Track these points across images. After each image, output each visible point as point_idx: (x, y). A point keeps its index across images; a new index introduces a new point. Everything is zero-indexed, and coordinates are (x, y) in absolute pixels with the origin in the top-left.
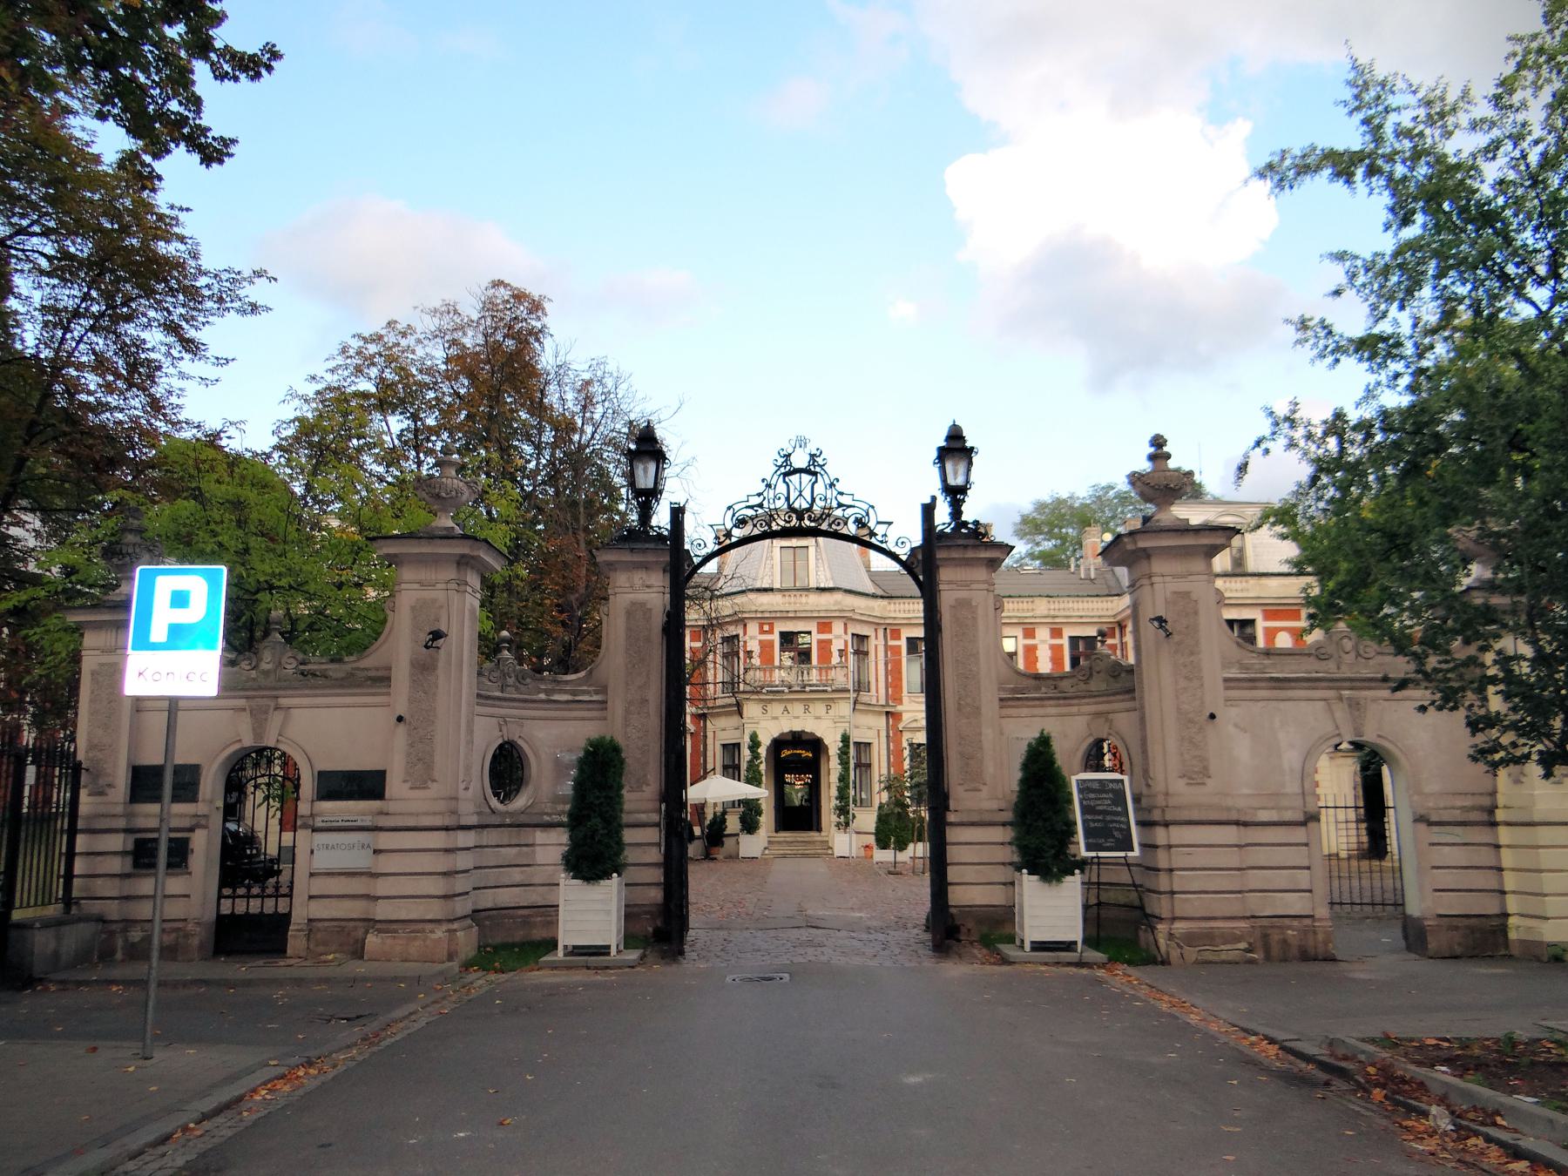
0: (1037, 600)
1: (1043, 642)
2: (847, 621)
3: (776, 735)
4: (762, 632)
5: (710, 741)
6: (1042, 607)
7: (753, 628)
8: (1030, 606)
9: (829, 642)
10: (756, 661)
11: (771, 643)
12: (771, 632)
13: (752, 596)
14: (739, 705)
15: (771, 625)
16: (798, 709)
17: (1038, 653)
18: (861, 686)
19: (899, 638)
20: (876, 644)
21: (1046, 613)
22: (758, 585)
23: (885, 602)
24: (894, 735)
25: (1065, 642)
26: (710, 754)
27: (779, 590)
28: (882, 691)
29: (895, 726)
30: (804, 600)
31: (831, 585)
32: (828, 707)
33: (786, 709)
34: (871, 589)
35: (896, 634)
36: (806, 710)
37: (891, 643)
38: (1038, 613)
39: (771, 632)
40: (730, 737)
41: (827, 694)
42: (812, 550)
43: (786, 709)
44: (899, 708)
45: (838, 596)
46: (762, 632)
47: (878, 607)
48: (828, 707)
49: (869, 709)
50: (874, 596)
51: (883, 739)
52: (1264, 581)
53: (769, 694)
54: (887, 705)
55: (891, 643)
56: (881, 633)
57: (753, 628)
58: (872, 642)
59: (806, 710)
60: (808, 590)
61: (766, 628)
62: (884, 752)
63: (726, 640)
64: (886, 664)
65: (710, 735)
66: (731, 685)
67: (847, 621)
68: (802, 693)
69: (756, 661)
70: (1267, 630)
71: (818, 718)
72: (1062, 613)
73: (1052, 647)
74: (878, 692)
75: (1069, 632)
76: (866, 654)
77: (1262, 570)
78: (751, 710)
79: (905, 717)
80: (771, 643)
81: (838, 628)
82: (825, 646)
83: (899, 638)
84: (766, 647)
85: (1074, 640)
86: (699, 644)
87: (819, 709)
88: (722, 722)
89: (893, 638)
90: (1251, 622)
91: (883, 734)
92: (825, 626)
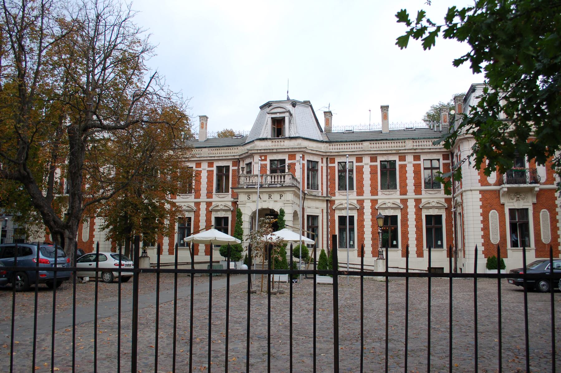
1: (410, 162)
6: (409, 145)
7: (257, 158)
8: (403, 144)
11: (266, 165)
12: (265, 160)
15: (266, 156)
17: (407, 169)
20: (322, 166)
21: (411, 147)
22: (260, 137)
23: (327, 145)
24: (330, 212)
28: (325, 189)
29: (331, 207)
30: (282, 143)
32: (281, 196)
35: (333, 161)
37: (330, 165)
38: (407, 148)
39: (265, 160)
44: (333, 198)
45: (299, 141)
46: (262, 160)
47: (323, 147)
48: (281, 196)
50: (322, 142)
51: (325, 214)
54: (327, 196)
56: (325, 160)
57: (257, 158)
58: (320, 165)
59: (270, 197)
62: (325, 220)
63: (247, 164)
64: (327, 176)
67: (304, 153)
72: (420, 147)
74: (322, 189)
76: (317, 171)
79: (337, 202)
80: (266, 165)
81: (298, 156)
84: (263, 167)
86: (236, 168)
87: (276, 197)
91: (325, 211)
92: (292, 156)
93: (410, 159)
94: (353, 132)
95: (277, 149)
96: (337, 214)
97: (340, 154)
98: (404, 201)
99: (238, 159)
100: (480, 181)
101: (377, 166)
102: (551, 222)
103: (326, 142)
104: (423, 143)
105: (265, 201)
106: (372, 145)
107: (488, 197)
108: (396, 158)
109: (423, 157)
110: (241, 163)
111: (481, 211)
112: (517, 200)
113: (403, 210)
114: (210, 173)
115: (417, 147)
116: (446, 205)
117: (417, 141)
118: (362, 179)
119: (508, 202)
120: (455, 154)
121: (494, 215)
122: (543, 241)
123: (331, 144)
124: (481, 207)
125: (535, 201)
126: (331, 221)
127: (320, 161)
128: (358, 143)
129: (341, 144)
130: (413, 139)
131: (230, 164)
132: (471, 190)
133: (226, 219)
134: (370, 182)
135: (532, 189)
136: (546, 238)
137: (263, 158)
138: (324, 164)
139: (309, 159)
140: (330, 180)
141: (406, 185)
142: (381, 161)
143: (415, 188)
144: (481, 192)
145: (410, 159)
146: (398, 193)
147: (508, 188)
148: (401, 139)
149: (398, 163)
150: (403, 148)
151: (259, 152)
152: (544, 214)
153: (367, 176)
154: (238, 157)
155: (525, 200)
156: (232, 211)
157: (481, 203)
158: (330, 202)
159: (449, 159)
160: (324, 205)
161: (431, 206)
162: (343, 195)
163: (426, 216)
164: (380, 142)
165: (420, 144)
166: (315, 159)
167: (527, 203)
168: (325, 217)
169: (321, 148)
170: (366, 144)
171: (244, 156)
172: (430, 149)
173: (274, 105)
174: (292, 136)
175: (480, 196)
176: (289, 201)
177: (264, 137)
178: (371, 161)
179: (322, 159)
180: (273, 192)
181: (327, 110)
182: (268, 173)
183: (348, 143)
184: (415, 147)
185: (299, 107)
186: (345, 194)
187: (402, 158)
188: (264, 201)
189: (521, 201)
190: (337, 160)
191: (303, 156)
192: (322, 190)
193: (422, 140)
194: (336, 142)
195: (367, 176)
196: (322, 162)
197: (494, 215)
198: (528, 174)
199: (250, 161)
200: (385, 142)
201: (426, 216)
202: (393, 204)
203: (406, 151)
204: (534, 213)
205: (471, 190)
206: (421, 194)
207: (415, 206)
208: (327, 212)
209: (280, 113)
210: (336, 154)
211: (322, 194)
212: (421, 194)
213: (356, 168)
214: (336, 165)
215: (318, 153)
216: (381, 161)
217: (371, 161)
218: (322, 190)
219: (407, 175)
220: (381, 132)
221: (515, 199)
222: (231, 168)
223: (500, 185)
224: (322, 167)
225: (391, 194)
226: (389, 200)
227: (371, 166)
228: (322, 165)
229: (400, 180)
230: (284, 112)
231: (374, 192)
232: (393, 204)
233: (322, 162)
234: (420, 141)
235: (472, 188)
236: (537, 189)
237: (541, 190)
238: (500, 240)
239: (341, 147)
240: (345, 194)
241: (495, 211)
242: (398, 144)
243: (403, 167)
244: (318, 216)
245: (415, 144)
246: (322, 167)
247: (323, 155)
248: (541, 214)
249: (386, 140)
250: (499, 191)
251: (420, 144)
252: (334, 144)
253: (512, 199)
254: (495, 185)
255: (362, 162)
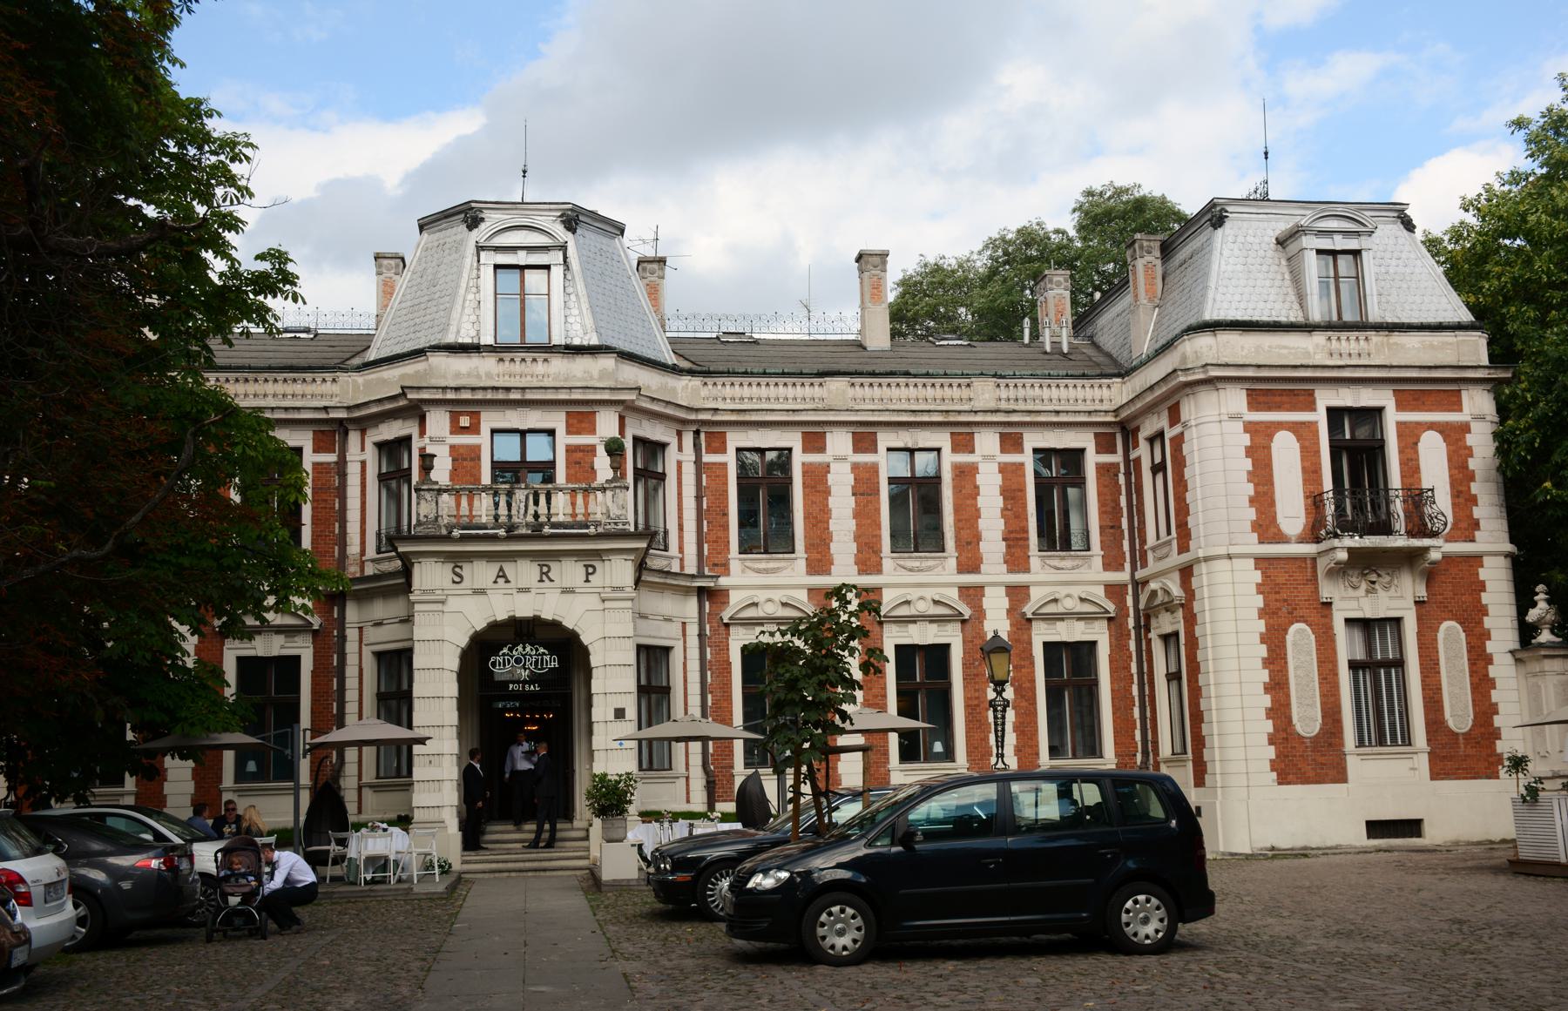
0: (978, 383)
1: (988, 458)
2: (626, 410)
3: (480, 625)
4: (457, 429)
5: (351, 647)
6: (985, 394)
7: (438, 422)
8: (965, 393)
9: (591, 450)
10: (441, 473)
12: (474, 429)
13: (438, 361)
14: (407, 572)
15: (475, 417)
16: (525, 572)
17: (980, 479)
18: (651, 536)
19: (723, 450)
20: (680, 459)
21: (992, 405)
22: (450, 339)
23: (696, 382)
24: (713, 634)
25: (1027, 459)
26: (351, 672)
27: (491, 349)
30: (540, 368)
31: (594, 341)
32: (590, 572)
33: (502, 574)
34: (671, 359)
36: (545, 575)
37: (708, 458)
38: (978, 405)
39: (474, 429)
40: (386, 637)
41: (586, 543)
42: (557, 272)
43: (502, 574)
44: (723, 581)
45: (608, 362)
46: (457, 429)
48: (590, 572)
49: (670, 583)
50: (675, 370)
51: (693, 641)
52: (1398, 338)
53: (463, 545)
55: (708, 458)
56: (688, 439)
58: (672, 454)
59: (545, 575)
60: (550, 349)
61: (465, 421)
64: (699, 498)
65: (352, 634)
66: (391, 540)
67: (626, 410)
68: (542, 543)
69: (441, 473)
70: (1401, 426)
71: (567, 591)
72: (1021, 406)
73: (1004, 469)
75: (1033, 440)
76: (662, 477)
77: (1390, 319)
78: (429, 575)
79: (736, 599)
81: (607, 424)
82: (580, 458)
83: (723, 450)
84: (465, 460)
85: (1044, 455)
86: (331, 458)
87: (570, 572)
88: (379, 609)
89: (710, 450)
90: (1378, 411)
91: (693, 630)
93: (839, 443)
94: (756, 342)
95: (523, 389)
96: (739, 639)
97: (747, 418)
98: (972, 594)
99: (340, 421)
100: (1257, 526)
101: (724, 465)
102: (1472, 663)
103: (691, 372)
104: (1030, 393)
105: (526, 590)
106: (858, 391)
107: (1281, 580)
108: (793, 440)
109: (885, 439)
110: (354, 438)
111: (1261, 626)
112: (1368, 591)
113: (968, 626)
114: (1011, 473)
115: (1012, 406)
116: (1111, 607)
117: (1012, 382)
118: (826, 512)
119: (1343, 598)
120: (1142, 435)
121: (1300, 637)
122: (1451, 724)
123: (710, 381)
124: (1262, 613)
125: (1422, 592)
126: (712, 667)
127: (673, 441)
128: (807, 381)
129: (746, 380)
130: (995, 376)
131: (1084, 440)
132: (1229, 557)
133: (940, 653)
134: (852, 524)
135: (1410, 558)
136: (1458, 715)
137: (465, 421)
138: (689, 454)
139: (641, 433)
140: (711, 516)
141: (978, 538)
142: (739, 450)
143: (1008, 547)
144: (1261, 562)
145: (839, 443)
146: (952, 563)
147: (1350, 550)
148: (955, 376)
149: (799, 459)
150: (966, 407)
151: (450, 396)
152: (1450, 633)
153: (990, 502)
154: (342, 415)
155: (1392, 592)
156: (315, 633)
157: (1259, 601)
158: (710, 596)
159: (1114, 451)
160: (691, 606)
161: (1061, 610)
162: (758, 571)
163: (1046, 644)
164: (885, 381)
165: (1021, 393)
166: (655, 432)
167: (1398, 598)
168: (694, 653)
169: (674, 389)
170: (837, 385)
171: (374, 409)
172: (1057, 412)
173: (492, 220)
174: (577, 342)
175: (1257, 576)
176: (621, 589)
177: (468, 340)
178: (856, 450)
179: (679, 434)
180: (558, 555)
181: (650, 254)
182: (486, 479)
183: (772, 380)
184: (1004, 405)
185: (587, 233)
186: (763, 565)
187: (814, 441)
188: (521, 590)
189: (1381, 593)
190: (735, 439)
191: (622, 419)
192: (681, 550)
193: (1028, 382)
194: (729, 373)
195: (990, 502)
196: (680, 449)
197: (1300, 637)
198: (1398, 507)
199: (403, 433)
200: (902, 381)
201: (1046, 644)
202: (784, 605)
203: (979, 418)
204: (1420, 635)
205: (1229, 557)
206: (1027, 570)
207: (1009, 611)
208: (701, 635)
209: (530, 249)
210: (734, 418)
211: (682, 567)
212: (1027, 570)
213: (805, 473)
214: (730, 458)
215: (670, 411)
216: (739, 450)
217: (856, 450)
218: (681, 550)
219: (981, 501)
220: (860, 345)
221: (1364, 586)
222: (1092, 460)
223: (1318, 540)
224: (679, 464)
225: (929, 569)
226: (917, 590)
227: (855, 467)
228: (680, 458)
229: (957, 521)
230: (545, 249)
231: (1016, 559)
232: (784, 605)
233: (680, 449)
234: (1020, 382)
235: (1233, 550)
236: (1435, 555)
237: (1447, 558)
238: (1324, 724)
239: (746, 392)
240: (763, 565)
241: (1453, 623)
242: (948, 392)
243: (965, 474)
244: (667, 650)
245: (1004, 396)
246: (679, 464)
247: (684, 422)
248: (1441, 635)
249: (907, 374)
250: (1314, 560)
251: (1021, 393)
252: (720, 381)
253: (1355, 588)
254: (1302, 540)
255: (971, 450)
